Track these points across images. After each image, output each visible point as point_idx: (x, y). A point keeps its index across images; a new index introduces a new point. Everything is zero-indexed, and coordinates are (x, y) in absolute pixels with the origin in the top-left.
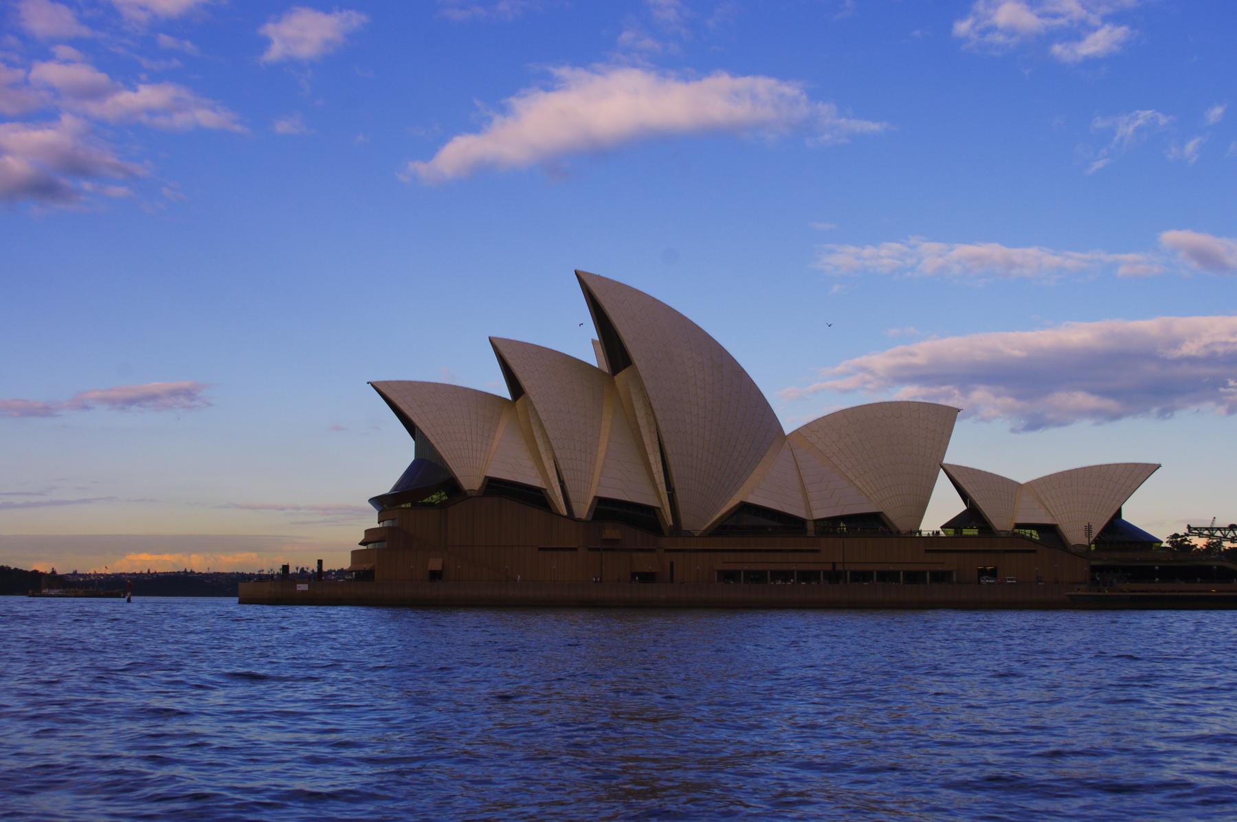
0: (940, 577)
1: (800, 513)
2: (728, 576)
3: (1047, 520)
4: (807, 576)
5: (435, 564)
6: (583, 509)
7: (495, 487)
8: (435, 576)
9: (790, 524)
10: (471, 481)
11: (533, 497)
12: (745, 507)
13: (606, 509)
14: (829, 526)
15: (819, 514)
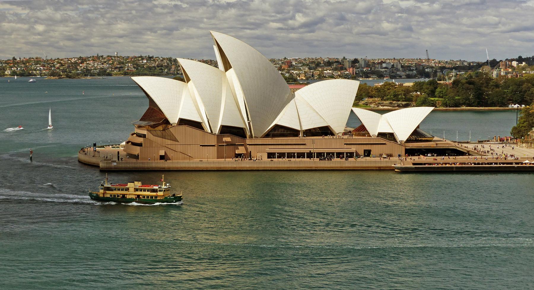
0: (350, 155)
1: (298, 128)
2: (271, 155)
3: (390, 131)
4: (301, 155)
5: (162, 153)
6: (217, 131)
7: (182, 122)
8: (162, 158)
9: (294, 133)
10: (174, 120)
11: (198, 125)
12: (277, 127)
13: (226, 130)
14: (310, 133)
15: (305, 128)
